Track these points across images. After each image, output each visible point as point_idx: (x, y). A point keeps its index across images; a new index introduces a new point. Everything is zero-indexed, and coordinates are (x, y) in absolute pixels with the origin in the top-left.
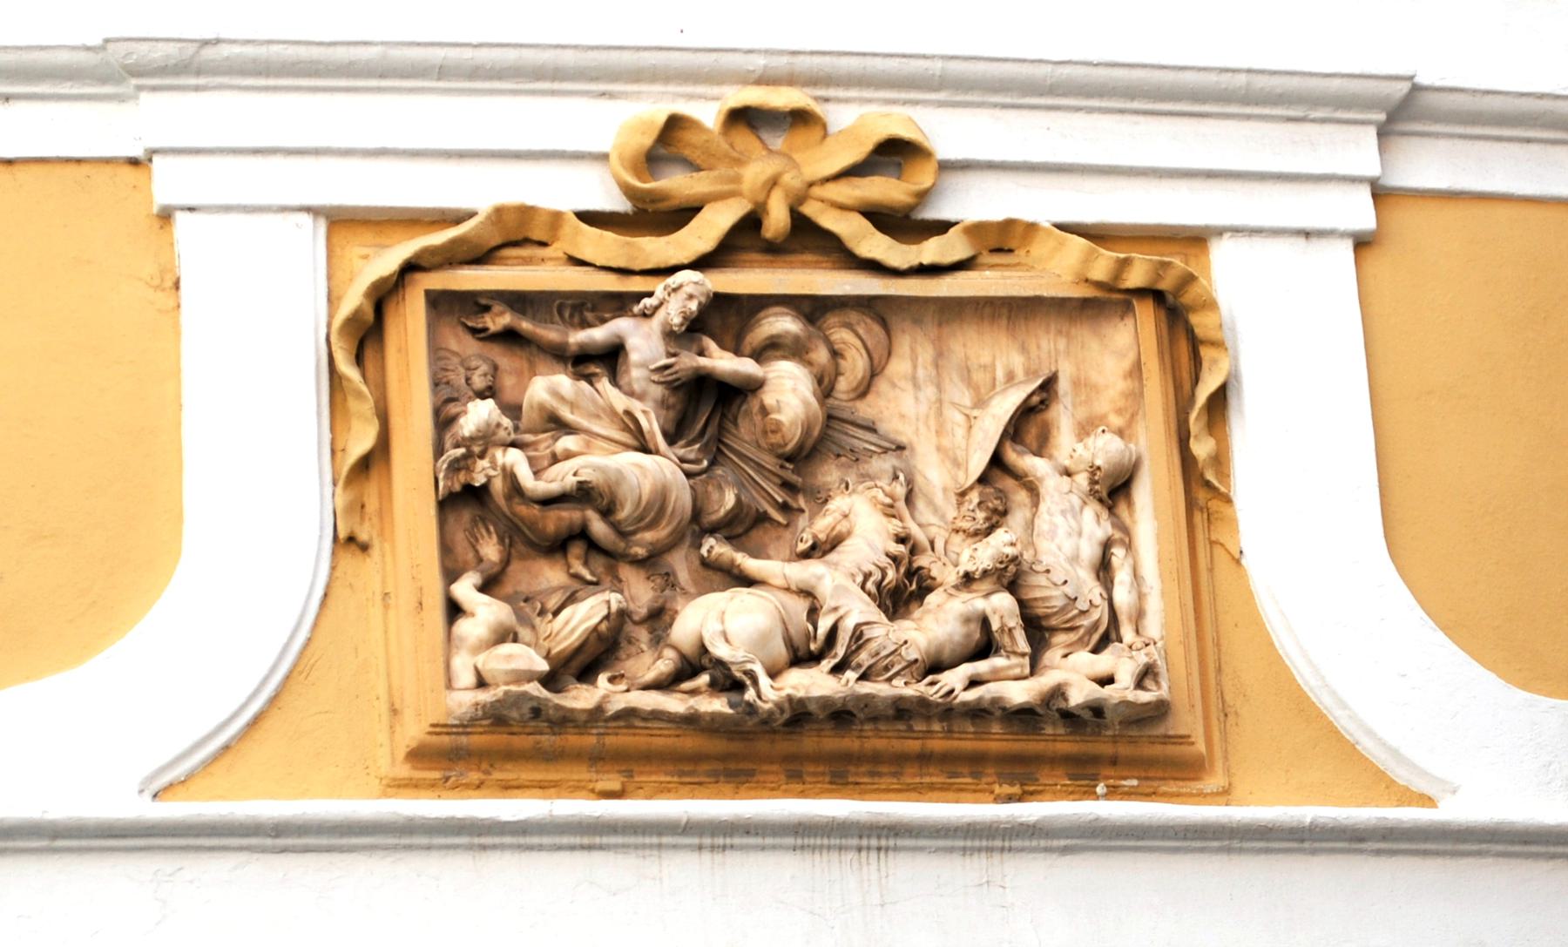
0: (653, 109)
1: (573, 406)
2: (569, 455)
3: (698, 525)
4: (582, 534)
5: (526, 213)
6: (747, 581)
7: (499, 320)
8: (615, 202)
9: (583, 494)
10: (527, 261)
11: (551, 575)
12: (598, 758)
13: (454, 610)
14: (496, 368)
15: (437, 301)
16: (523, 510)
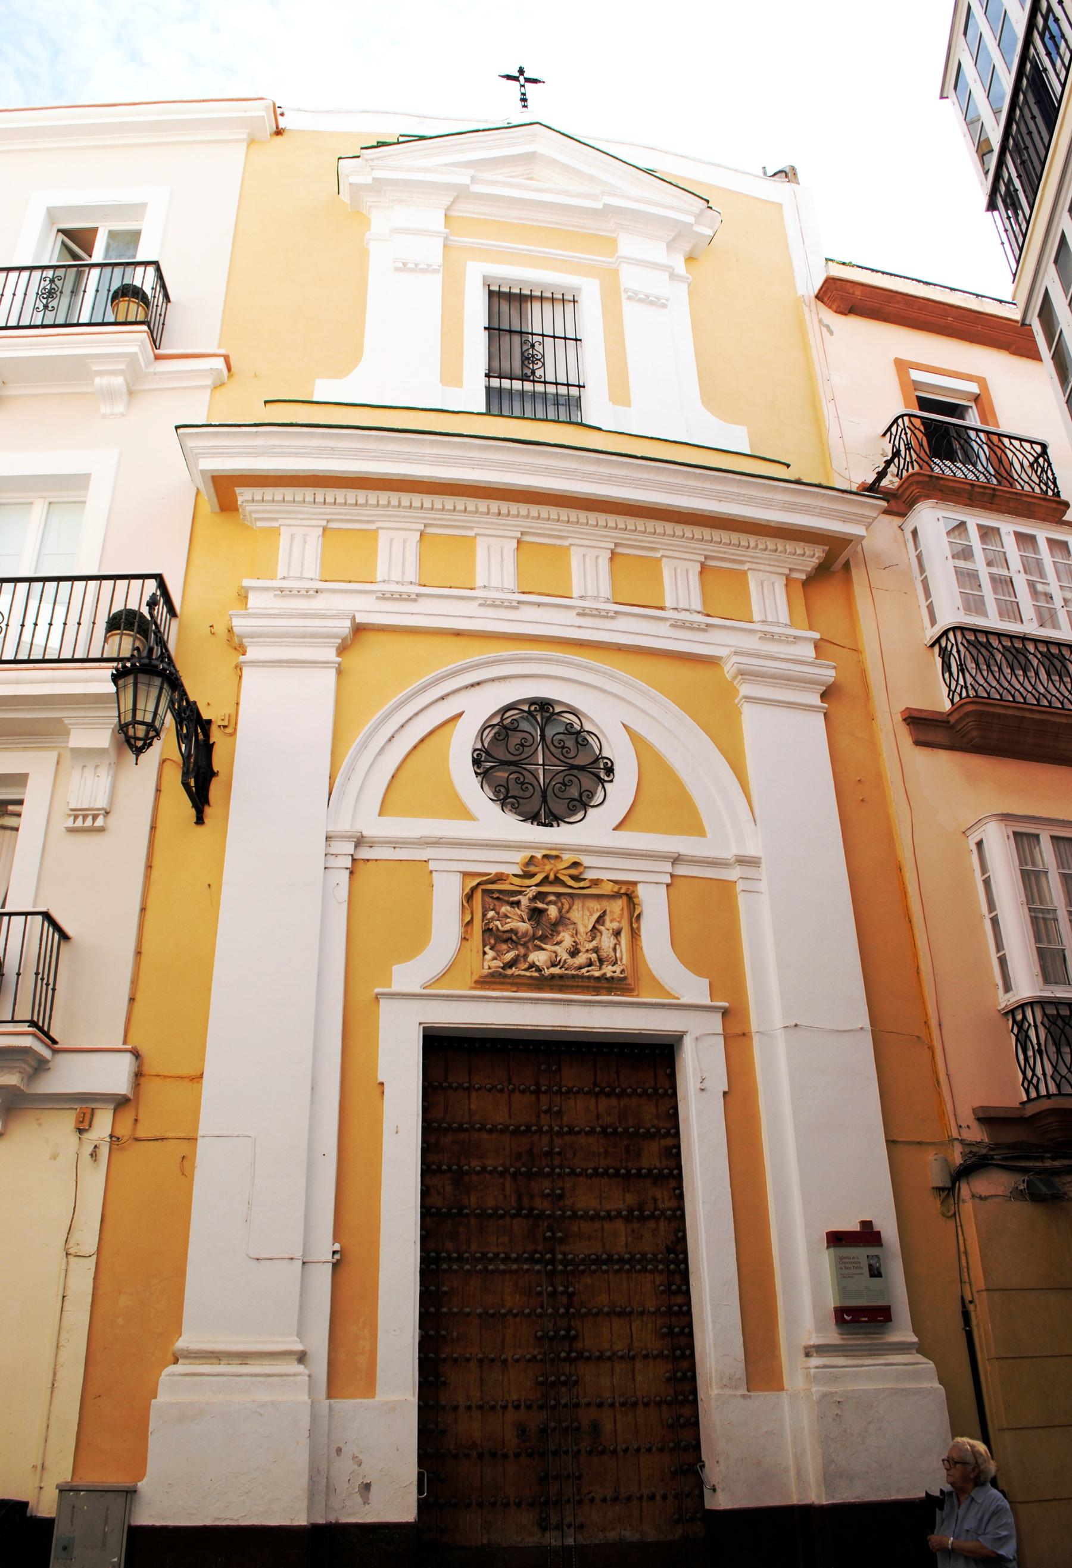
0: (528, 854)
1: (510, 913)
2: (509, 923)
3: (534, 937)
4: (511, 939)
5: (502, 874)
6: (544, 949)
7: (496, 895)
8: (521, 873)
9: (511, 931)
10: (502, 884)
11: (504, 947)
12: (512, 984)
13: (485, 953)
14: (495, 905)
15: (484, 891)
16: (499, 934)
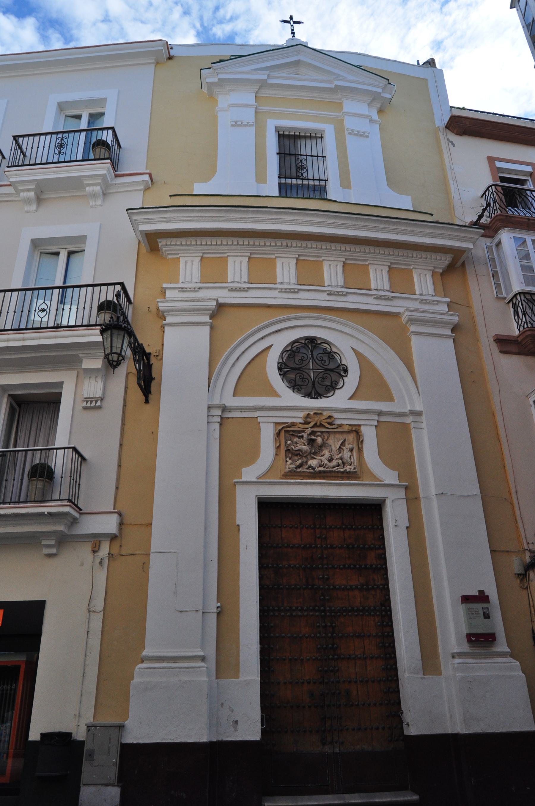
0: (306, 413)
1: (298, 441)
2: (298, 446)
3: (310, 453)
4: (299, 454)
5: (294, 423)
6: (315, 459)
7: (291, 433)
8: (303, 422)
9: (299, 450)
10: (294, 427)
11: (296, 458)
12: (300, 476)
13: (287, 461)
14: (291, 438)
15: (285, 431)
16: (293, 451)
